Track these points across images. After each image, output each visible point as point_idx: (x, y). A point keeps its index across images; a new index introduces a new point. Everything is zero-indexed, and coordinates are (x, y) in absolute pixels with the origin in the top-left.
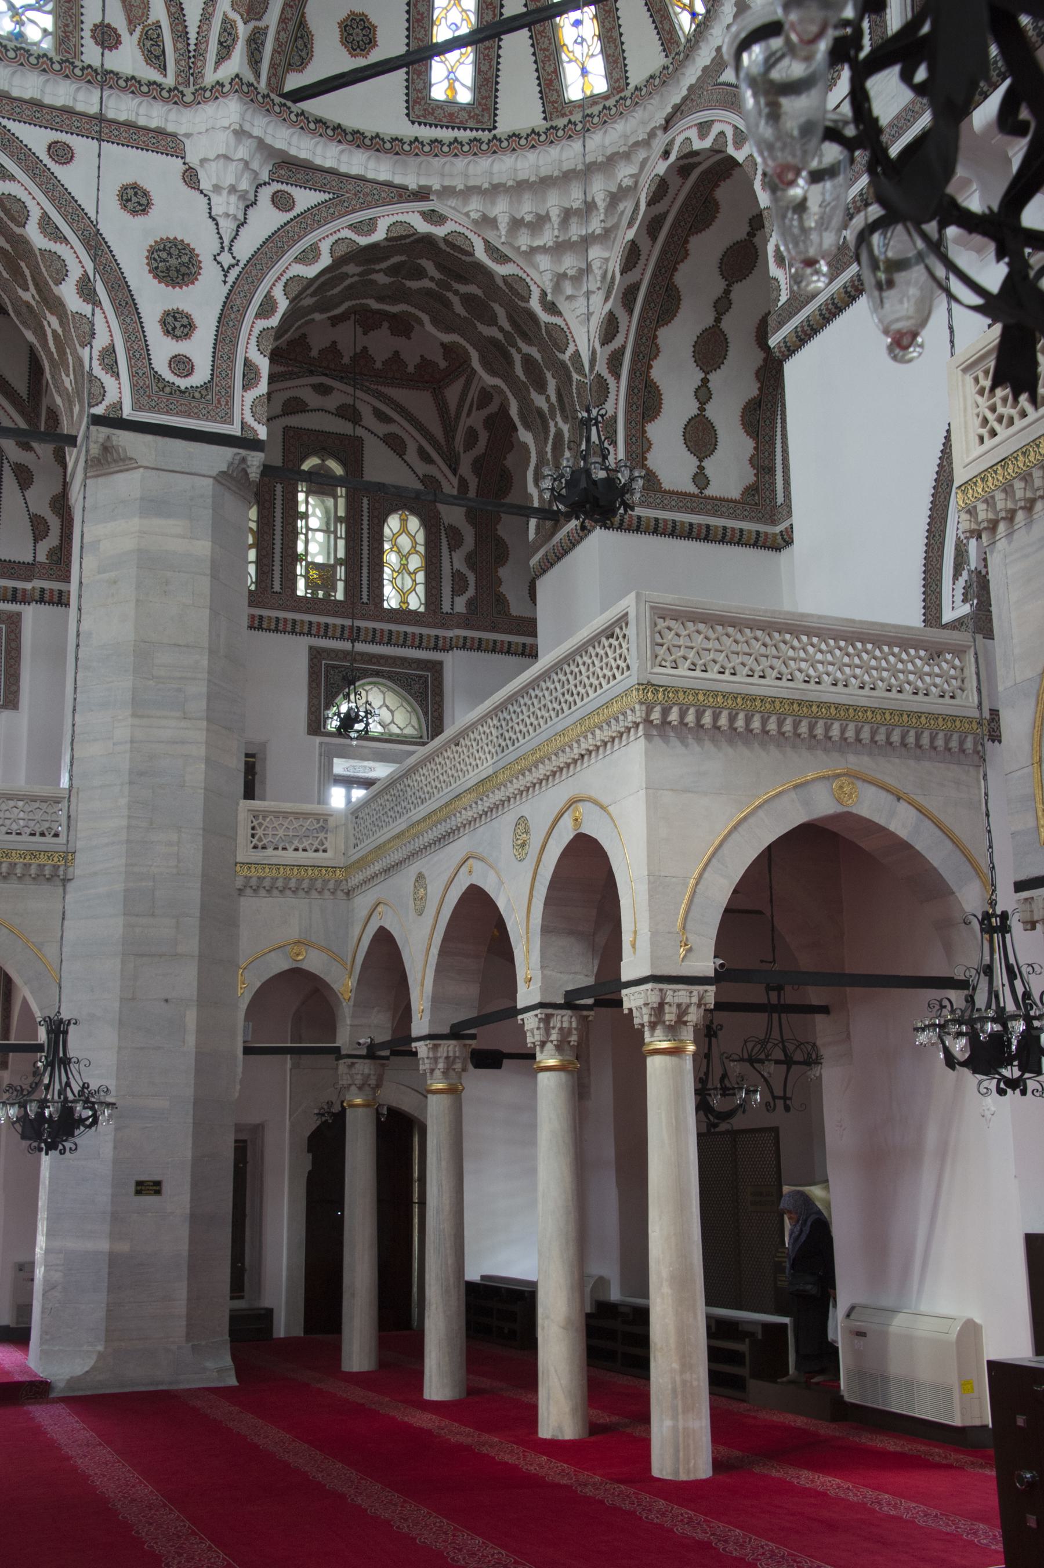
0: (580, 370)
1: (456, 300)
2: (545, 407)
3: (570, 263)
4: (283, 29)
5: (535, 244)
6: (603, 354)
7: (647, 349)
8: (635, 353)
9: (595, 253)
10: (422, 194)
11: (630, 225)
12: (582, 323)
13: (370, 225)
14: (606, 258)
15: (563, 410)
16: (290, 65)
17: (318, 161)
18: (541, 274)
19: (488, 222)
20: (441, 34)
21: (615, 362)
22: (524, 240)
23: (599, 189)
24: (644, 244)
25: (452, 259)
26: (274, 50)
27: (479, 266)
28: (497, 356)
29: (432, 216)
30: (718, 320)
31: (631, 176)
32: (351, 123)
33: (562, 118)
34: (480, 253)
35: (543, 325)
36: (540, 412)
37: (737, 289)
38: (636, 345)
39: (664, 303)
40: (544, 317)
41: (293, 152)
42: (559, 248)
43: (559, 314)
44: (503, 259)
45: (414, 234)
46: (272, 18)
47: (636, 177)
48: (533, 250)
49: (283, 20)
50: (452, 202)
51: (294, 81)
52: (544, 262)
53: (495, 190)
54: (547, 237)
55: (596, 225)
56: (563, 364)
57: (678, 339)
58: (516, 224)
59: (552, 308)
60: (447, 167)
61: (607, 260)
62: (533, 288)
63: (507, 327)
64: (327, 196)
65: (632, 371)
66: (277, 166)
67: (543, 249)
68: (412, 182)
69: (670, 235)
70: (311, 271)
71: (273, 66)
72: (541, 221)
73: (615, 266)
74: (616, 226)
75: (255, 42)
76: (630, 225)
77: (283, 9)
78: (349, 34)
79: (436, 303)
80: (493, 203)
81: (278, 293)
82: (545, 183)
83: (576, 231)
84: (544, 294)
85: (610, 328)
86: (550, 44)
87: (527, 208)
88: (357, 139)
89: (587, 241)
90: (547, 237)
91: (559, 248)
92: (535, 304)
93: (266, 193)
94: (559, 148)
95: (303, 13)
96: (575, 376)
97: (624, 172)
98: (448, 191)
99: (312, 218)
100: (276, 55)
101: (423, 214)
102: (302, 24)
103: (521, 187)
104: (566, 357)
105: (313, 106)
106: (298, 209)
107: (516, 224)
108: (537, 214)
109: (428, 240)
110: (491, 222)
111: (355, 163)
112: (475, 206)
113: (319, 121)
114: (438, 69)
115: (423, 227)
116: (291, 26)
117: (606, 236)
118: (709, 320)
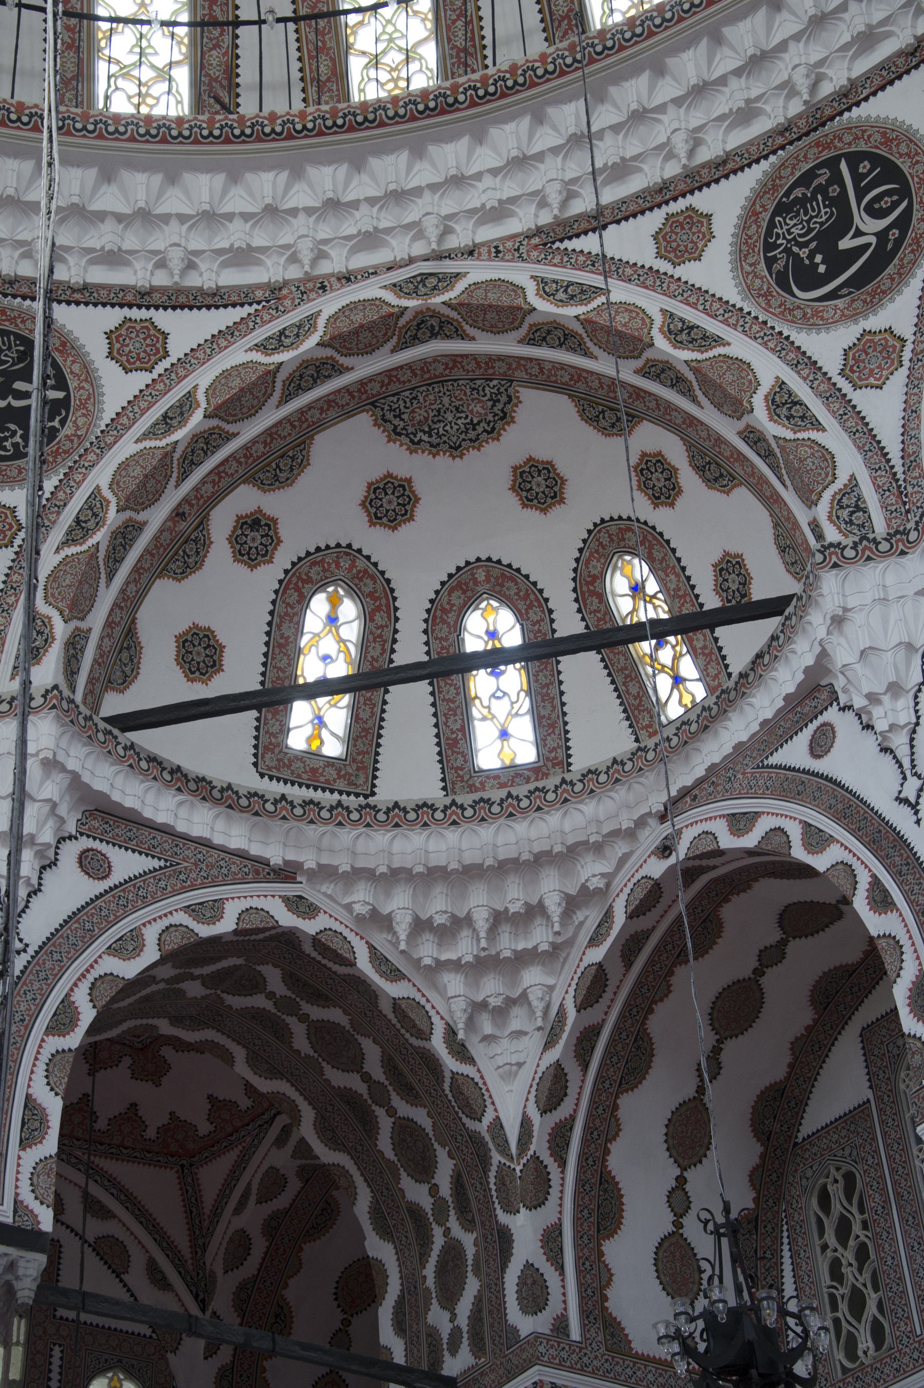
0: (503, 1147)
1: (299, 1030)
2: (427, 1203)
3: (492, 988)
4: (108, 635)
5: (444, 957)
6: (541, 1125)
7: (604, 1127)
8: (588, 1129)
9: (533, 977)
10: (287, 873)
11: (594, 942)
12: (509, 1078)
13: (214, 910)
14: (553, 988)
15: (463, 1209)
16: (110, 681)
17: (148, 813)
18: (448, 1002)
19: (379, 920)
20: (310, 669)
21: (559, 1139)
22: (428, 951)
23: (551, 889)
24: (614, 972)
25: (310, 969)
26: (95, 660)
27: (360, 984)
28: (349, 1119)
29: (297, 904)
31: (603, 875)
32: (193, 766)
33: (468, 793)
34: (364, 963)
35: (448, 1075)
36: (415, 1212)
37: (729, 1046)
38: (590, 1117)
39: (630, 1060)
40: (451, 1064)
41: (116, 797)
42: (483, 965)
43: (471, 1061)
44: (395, 975)
45: (273, 928)
46: (97, 619)
47: (609, 878)
48: (440, 965)
49: (109, 624)
50: (328, 888)
51: (115, 704)
52: (454, 983)
53: (396, 876)
54: (464, 948)
55: (540, 937)
56: (475, 1139)
57: (645, 1113)
58: (420, 926)
59: (461, 1052)
60: (326, 839)
61: (551, 988)
62: (436, 1019)
63: (378, 1074)
65: (583, 1157)
66: (90, 814)
67: (456, 965)
68: (275, 854)
69: (651, 962)
70: (130, 969)
71: (91, 681)
72: (459, 923)
73: (566, 997)
74: (570, 943)
75: (74, 646)
76: (594, 942)
77: (112, 610)
78: (187, 652)
79: (265, 1038)
80: (388, 895)
81: (81, 998)
82: (471, 873)
83: (508, 944)
84: (451, 1032)
85: (553, 1090)
86: (458, 694)
87: (438, 905)
88: (201, 788)
89: (523, 959)
90: (464, 948)
91: (483, 965)
92: (438, 1043)
93: (70, 852)
94: (493, 828)
95: (135, 619)
96: (496, 1158)
97: (591, 870)
98: (326, 872)
99: (133, 893)
100: (96, 666)
101: (286, 900)
102: (130, 632)
103: (435, 875)
104: (483, 1127)
105: (149, 740)
106: (116, 878)
107: (420, 926)
108: (453, 916)
109: (290, 938)
110: (383, 921)
111: (199, 821)
112: (362, 897)
113: (153, 759)
114: (301, 711)
115: (286, 919)
116: (117, 631)
117: (553, 955)
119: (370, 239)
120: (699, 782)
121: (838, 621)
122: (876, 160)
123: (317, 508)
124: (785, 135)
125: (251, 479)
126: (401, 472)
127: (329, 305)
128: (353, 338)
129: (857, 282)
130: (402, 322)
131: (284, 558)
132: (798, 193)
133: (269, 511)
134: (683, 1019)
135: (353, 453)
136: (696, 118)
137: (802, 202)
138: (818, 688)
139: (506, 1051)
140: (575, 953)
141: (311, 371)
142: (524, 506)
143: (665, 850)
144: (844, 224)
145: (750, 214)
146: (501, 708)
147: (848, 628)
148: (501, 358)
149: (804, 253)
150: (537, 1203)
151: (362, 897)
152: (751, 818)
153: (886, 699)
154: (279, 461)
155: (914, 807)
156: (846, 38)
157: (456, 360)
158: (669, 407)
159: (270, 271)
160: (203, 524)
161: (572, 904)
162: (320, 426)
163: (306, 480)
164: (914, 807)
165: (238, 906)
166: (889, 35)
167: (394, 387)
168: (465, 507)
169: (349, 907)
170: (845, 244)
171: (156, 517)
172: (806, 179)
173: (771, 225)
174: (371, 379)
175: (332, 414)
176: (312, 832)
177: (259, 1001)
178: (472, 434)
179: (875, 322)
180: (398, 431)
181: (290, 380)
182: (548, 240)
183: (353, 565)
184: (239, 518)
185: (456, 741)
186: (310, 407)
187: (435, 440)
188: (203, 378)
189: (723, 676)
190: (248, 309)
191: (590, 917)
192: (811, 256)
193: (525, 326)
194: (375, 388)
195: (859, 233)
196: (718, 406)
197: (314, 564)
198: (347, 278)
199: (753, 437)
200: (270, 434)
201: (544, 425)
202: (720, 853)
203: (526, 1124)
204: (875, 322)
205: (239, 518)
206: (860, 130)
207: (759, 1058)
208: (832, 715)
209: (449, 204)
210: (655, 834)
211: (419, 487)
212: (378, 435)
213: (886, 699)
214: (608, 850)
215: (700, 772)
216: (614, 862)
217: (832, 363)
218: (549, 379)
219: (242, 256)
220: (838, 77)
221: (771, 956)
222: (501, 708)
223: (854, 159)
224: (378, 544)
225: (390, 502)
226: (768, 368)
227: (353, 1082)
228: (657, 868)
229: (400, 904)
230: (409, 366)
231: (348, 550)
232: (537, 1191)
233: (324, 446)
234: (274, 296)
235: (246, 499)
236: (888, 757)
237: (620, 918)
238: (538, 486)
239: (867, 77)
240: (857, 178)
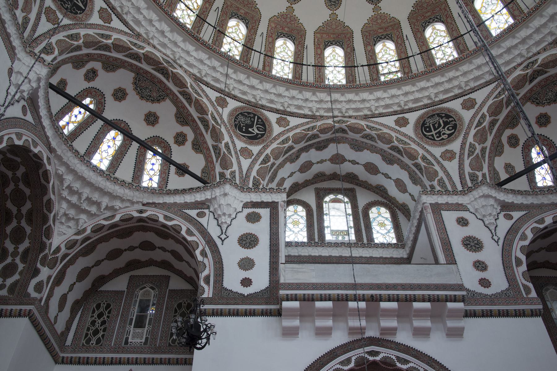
0: (50, 250)
3: (72, 212)
5: (67, 198)
7: (72, 262)
9: (83, 217)
11: (105, 219)
12: (61, 236)
18: (60, 208)
19: (61, 178)
22: (65, 194)
29: (48, 159)
30: (93, 267)
35: (48, 224)
43: (54, 225)
47: (120, 208)
48: (65, 199)
50: (56, 162)
52: (64, 205)
54: (74, 199)
55: (93, 209)
58: (69, 187)
60: (65, 151)
61: (85, 222)
64: (33, 123)
65: (65, 264)
67: (68, 202)
69: (112, 232)
80: (67, 174)
85: (71, 245)
90: (74, 199)
94: (102, 179)
96: (47, 251)
97: (117, 204)
98: (59, 158)
104: (48, 242)
108: (78, 191)
112: (62, 170)
118: (91, 265)
119: (164, 45)
120: (159, 204)
121: (225, 195)
122: (262, 121)
123: (107, 82)
124: (248, 103)
125: (103, 63)
126: (128, 91)
127: (148, 49)
128: (149, 59)
129: (250, 138)
130: (160, 65)
131: (92, 84)
132: (246, 114)
133: (99, 73)
134: (103, 250)
135: (124, 79)
136: (236, 85)
137: (246, 116)
138: (205, 204)
139: (63, 229)
140: (97, 219)
141: (136, 56)
142: (144, 120)
143: (141, 212)
144: (252, 126)
145: (236, 109)
146: (104, 155)
147: (226, 197)
148: (170, 90)
149: (242, 125)
150: (51, 268)
151: (62, 170)
152: (171, 219)
153: (227, 216)
154: (111, 66)
155: (223, 241)
156: (269, 98)
157: (161, 82)
158: (199, 128)
159: (141, 31)
160: (87, 62)
161: (107, 208)
162: (125, 67)
163: (111, 74)
164: (223, 241)
165: (39, 149)
166: (275, 104)
167: (144, 75)
168: (132, 111)
169: (57, 170)
170: (250, 130)
171: (85, 51)
172: (249, 113)
173: (238, 115)
174: (143, 69)
175: (129, 68)
176: (64, 147)
177: (10, 174)
178: (148, 98)
179: (250, 147)
180: (136, 84)
181: (131, 54)
182: (198, 80)
183: (101, 99)
184: (93, 68)
185: (90, 153)
186: (128, 62)
187: (140, 92)
188: (115, 36)
189: (164, 186)
190: (131, 32)
191: (108, 214)
192: (243, 126)
193: (183, 89)
194: (141, 71)
195: (253, 130)
196: (212, 137)
197: (95, 91)
198: (154, 47)
199: (216, 148)
200: (116, 59)
201: (166, 110)
202: (157, 221)
203: (58, 249)
204: (250, 147)
205: (93, 68)
206: (262, 114)
207: (107, 268)
208: (206, 211)
209: (183, 55)
210: (141, 207)
211: (128, 98)
212: (132, 80)
213: (227, 216)
214: (124, 203)
215: (161, 202)
216: (124, 206)
217: (238, 148)
218: (176, 102)
219: (138, 22)
220: (264, 102)
221: (132, 248)
222: (104, 155)
223: (259, 118)
224: (109, 100)
225: (120, 95)
226: (227, 139)
227: (14, 210)
228: (136, 214)
229: (69, 178)
230: (152, 74)
231: (103, 95)
232: (52, 266)
233: (121, 71)
234: (138, 36)
235: (97, 65)
236: (219, 228)
237: (117, 218)
238: (151, 119)
239: (268, 107)
240: (258, 121)
